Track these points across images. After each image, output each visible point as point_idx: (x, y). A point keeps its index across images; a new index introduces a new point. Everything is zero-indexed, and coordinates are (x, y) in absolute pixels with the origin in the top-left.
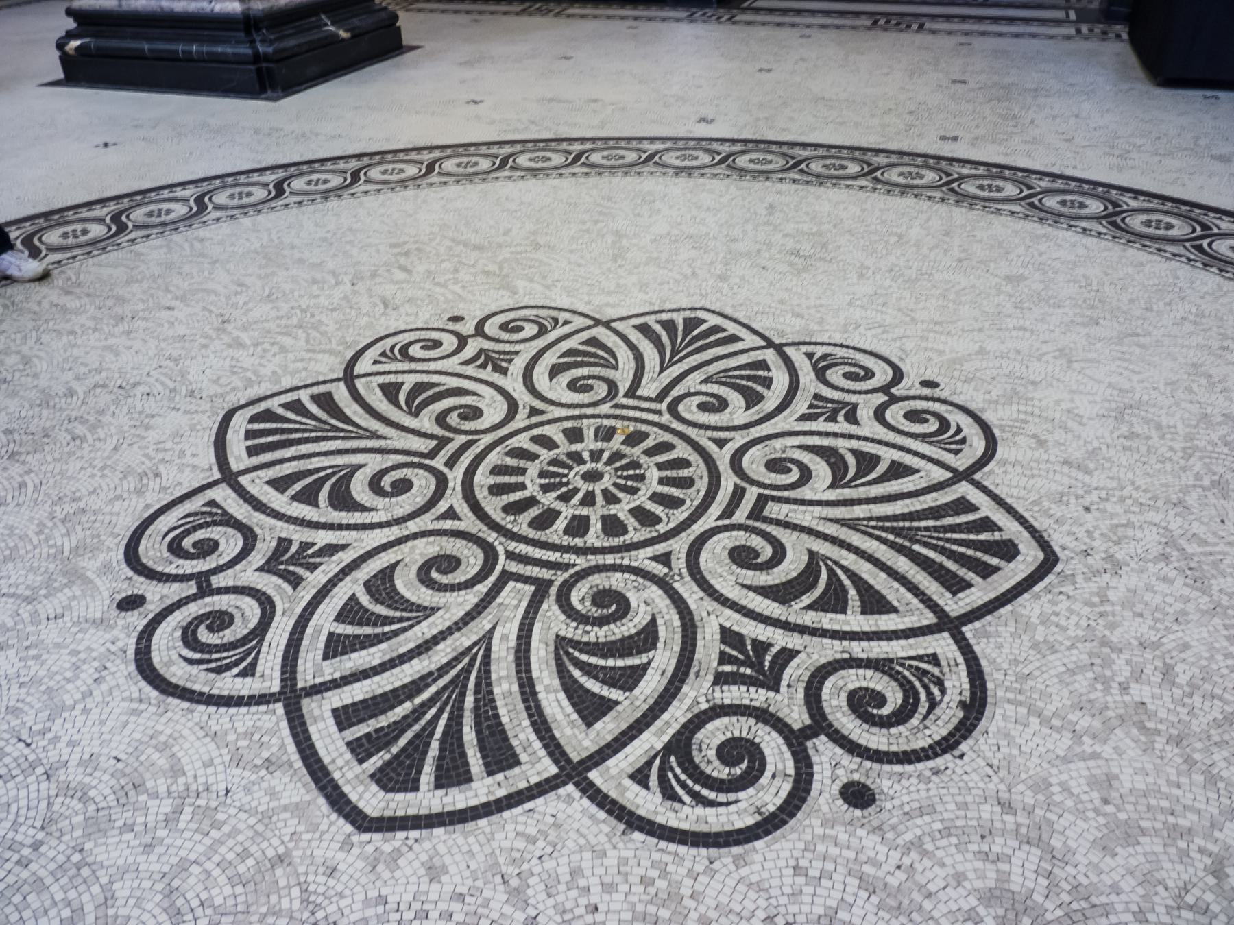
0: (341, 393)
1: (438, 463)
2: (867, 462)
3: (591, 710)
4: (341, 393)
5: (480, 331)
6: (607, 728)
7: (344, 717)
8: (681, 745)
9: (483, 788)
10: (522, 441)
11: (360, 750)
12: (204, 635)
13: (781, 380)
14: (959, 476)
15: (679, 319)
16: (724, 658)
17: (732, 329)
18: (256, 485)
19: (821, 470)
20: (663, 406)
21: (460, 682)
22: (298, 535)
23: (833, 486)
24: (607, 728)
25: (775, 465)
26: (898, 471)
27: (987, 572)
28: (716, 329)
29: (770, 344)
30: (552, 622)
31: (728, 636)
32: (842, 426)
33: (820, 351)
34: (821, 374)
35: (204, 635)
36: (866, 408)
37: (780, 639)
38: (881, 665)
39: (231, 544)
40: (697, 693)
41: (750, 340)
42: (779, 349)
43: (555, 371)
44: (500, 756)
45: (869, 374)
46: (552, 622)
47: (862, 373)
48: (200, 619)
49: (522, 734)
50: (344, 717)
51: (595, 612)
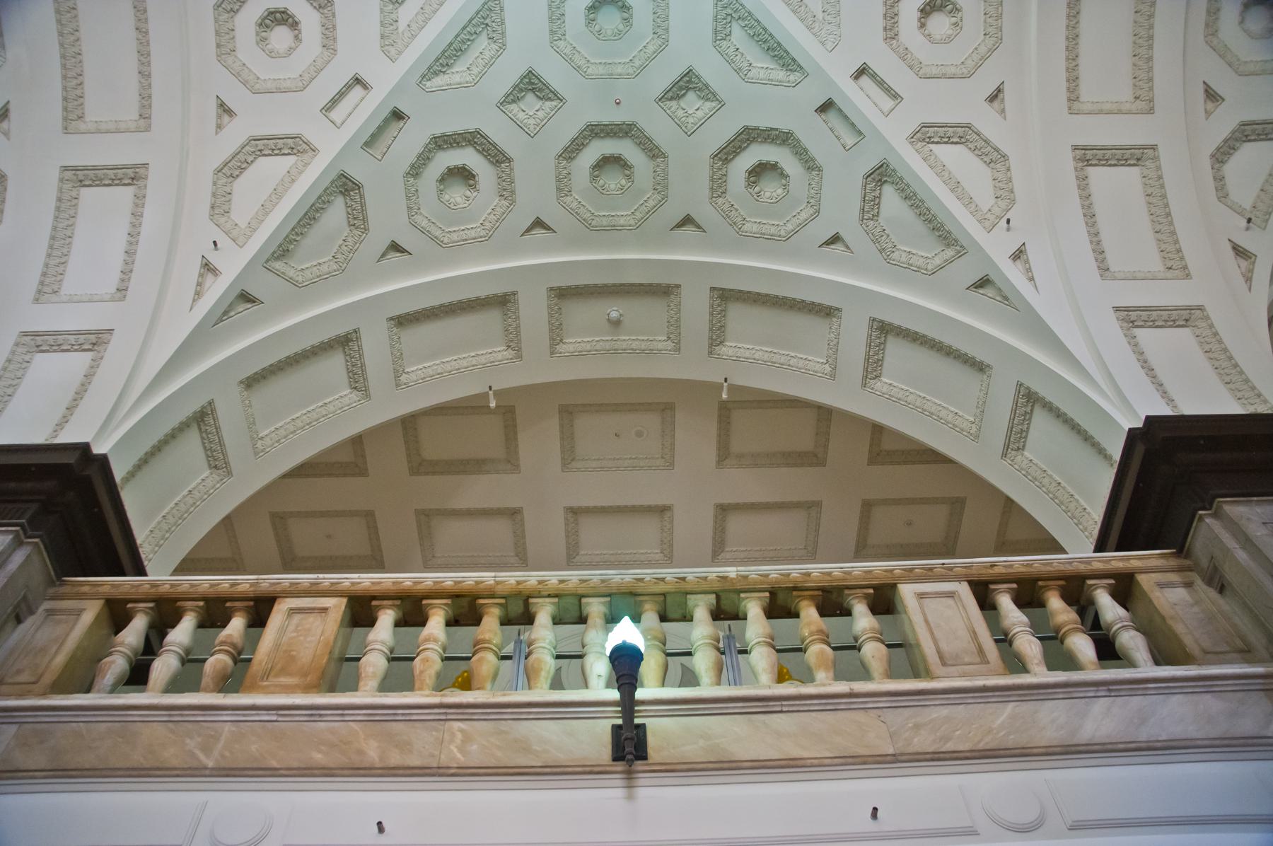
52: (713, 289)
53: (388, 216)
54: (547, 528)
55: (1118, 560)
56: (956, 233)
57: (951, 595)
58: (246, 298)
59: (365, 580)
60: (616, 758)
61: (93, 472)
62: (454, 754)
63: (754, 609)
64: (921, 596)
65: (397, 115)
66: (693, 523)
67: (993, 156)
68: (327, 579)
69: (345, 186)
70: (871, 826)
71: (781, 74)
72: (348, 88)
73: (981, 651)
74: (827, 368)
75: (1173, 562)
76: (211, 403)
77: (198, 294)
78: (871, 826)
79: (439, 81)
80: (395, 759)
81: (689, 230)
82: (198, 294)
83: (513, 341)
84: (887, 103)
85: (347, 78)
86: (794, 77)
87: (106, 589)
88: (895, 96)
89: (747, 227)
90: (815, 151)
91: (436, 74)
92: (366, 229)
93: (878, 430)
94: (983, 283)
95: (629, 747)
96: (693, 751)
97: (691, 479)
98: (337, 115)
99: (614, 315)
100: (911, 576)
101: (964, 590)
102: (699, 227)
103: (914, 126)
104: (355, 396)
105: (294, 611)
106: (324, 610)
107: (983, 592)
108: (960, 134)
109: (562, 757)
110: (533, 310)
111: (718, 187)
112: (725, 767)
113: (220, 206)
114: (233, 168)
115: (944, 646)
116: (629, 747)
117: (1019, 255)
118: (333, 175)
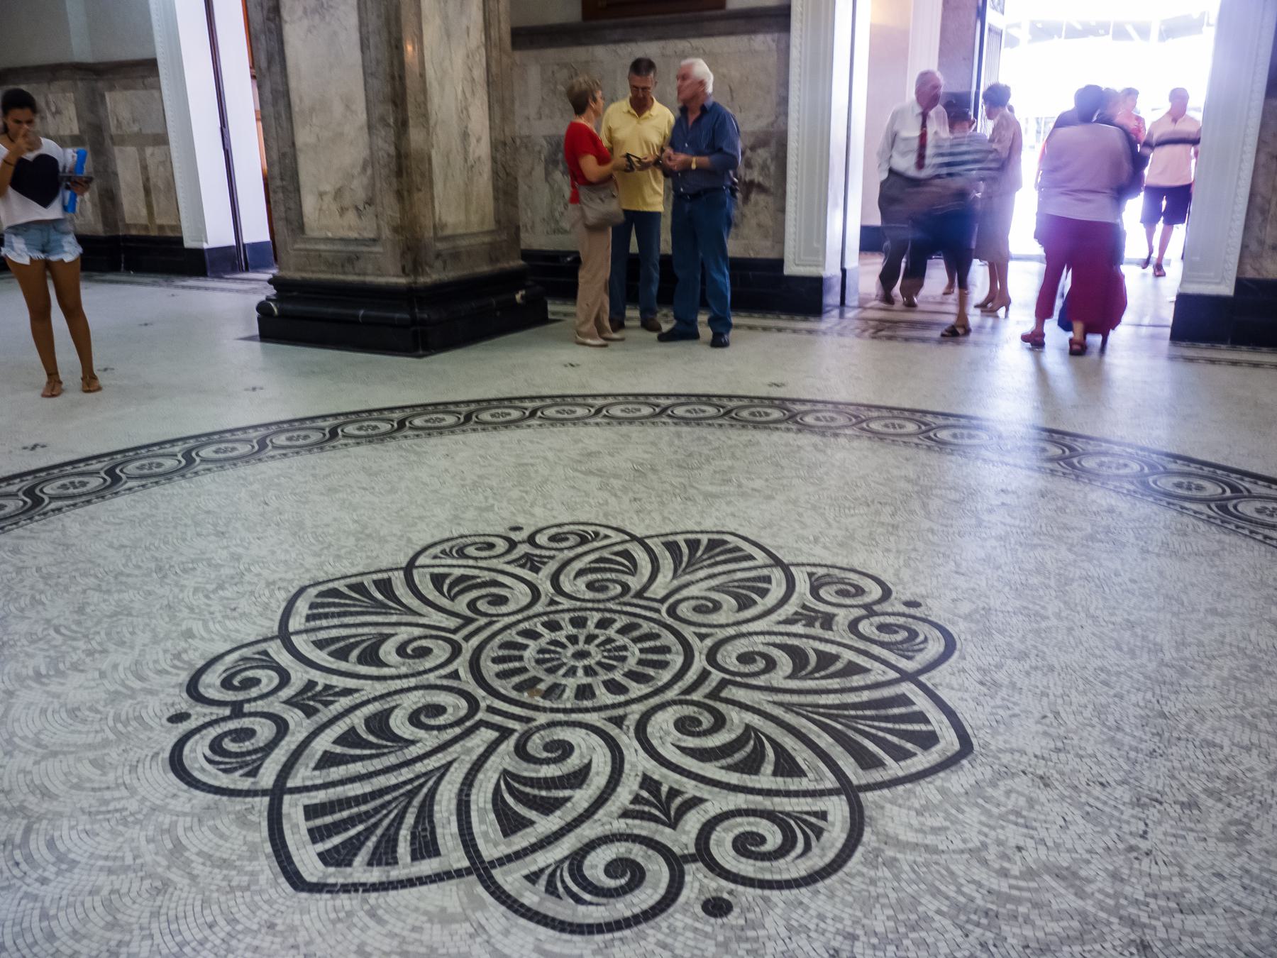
0: (398, 579)
1: (457, 637)
2: (826, 660)
3: (510, 824)
4: (398, 579)
5: (531, 540)
6: (521, 840)
7: (311, 812)
8: (577, 859)
9: (406, 867)
10: (637, 689)
11: (316, 835)
12: (229, 745)
14: (905, 676)
15: (704, 539)
16: (637, 799)
18: (299, 642)
19: (785, 663)
20: (664, 608)
21: (411, 794)
22: (321, 679)
23: (791, 676)
24: (521, 840)
26: (852, 669)
27: (900, 755)
30: (504, 758)
31: (648, 782)
33: (821, 571)
34: (814, 591)
35: (229, 745)
36: (843, 617)
37: (691, 788)
38: (770, 815)
39: (268, 679)
40: (607, 821)
41: (761, 558)
43: (580, 573)
44: (426, 846)
46: (504, 758)
47: (852, 590)
48: (225, 734)
49: (447, 833)
50: (311, 812)
51: (545, 755)
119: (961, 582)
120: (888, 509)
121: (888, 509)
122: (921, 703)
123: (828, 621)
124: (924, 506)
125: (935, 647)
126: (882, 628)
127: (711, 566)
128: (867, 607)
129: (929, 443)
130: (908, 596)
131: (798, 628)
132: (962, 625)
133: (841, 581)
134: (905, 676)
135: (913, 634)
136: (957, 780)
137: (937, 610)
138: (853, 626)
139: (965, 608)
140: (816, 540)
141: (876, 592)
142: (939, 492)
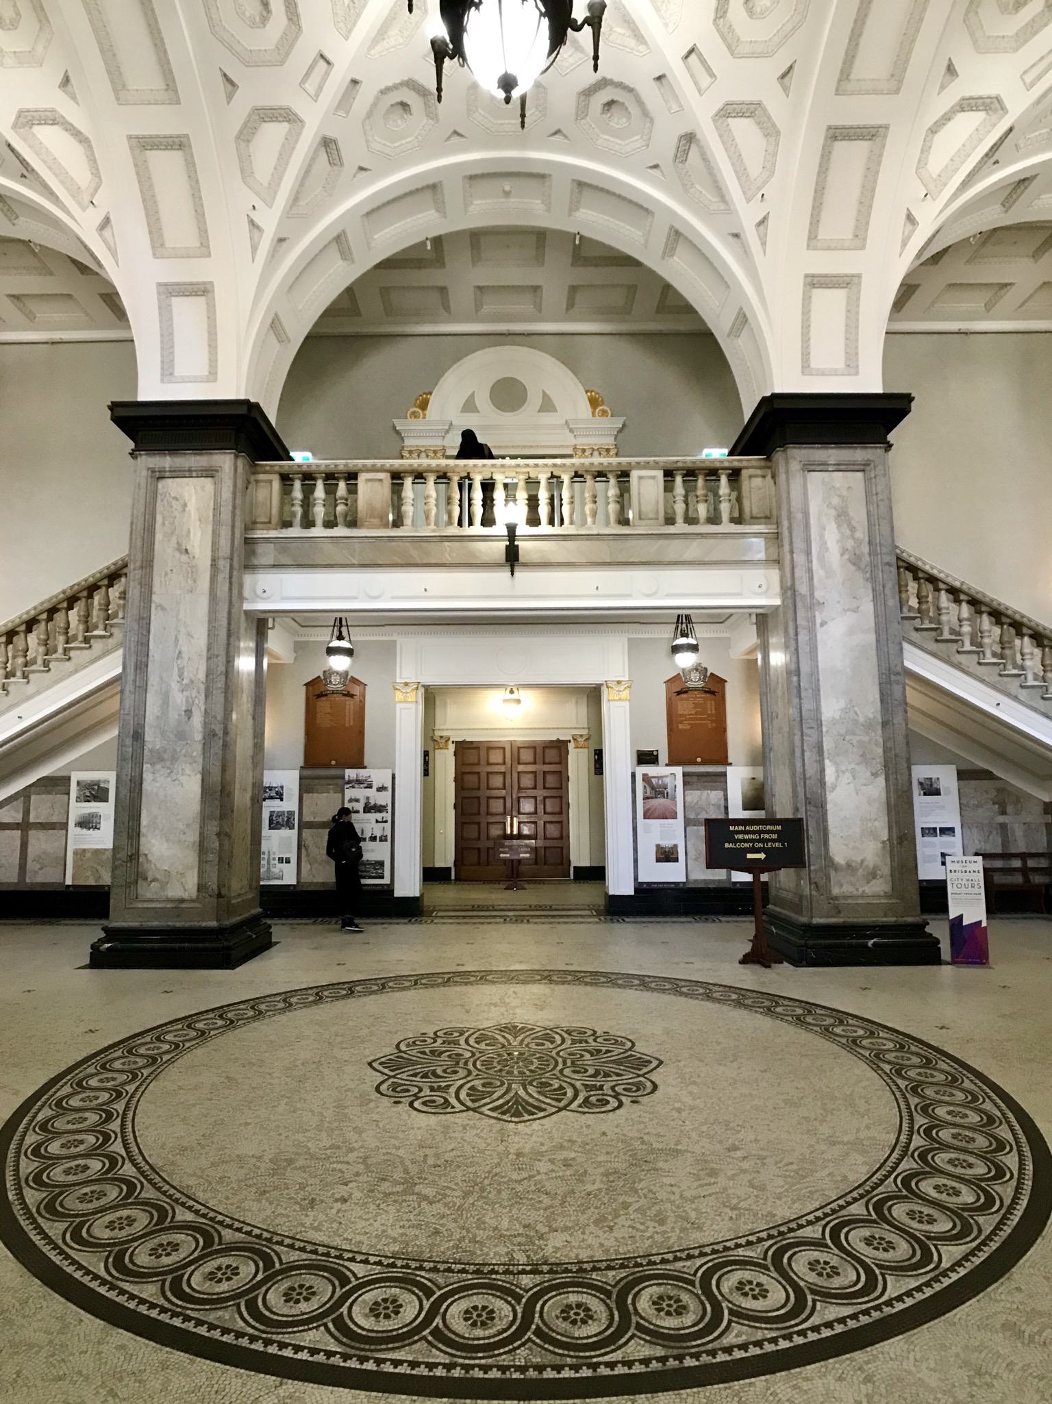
2: (425, 1076)
13: (463, 1095)
17: (495, 1115)
25: (456, 1072)
28: (504, 1113)
29: (474, 1110)
32: (435, 1085)
33: (449, 1110)
34: (446, 1100)
41: (484, 1109)
42: (468, 1109)
45: (424, 1103)
52: (573, 180)
53: (352, 153)
54: (462, 296)
55: (737, 461)
56: (727, 198)
57: (654, 478)
58: (281, 240)
59: (397, 463)
60: (507, 560)
61: (255, 414)
62: (449, 560)
63: (566, 478)
64: (640, 478)
65: (355, 82)
66: (554, 294)
67: (770, 131)
68: (379, 462)
69: (327, 143)
70: (596, 592)
71: (632, 43)
72: (315, 62)
73: (657, 512)
74: (642, 241)
75: (763, 463)
76: (276, 315)
77: (254, 249)
78: (596, 592)
79: (378, 48)
80: (425, 561)
81: (558, 138)
82: (254, 249)
83: (440, 207)
84: (705, 81)
85: (314, 54)
86: (642, 48)
87: (277, 469)
88: (712, 75)
89: (599, 142)
90: (650, 105)
91: (378, 42)
92: (342, 165)
93: (667, 288)
94: (736, 236)
95: (512, 557)
96: (535, 558)
97: (553, 277)
98: (310, 86)
99: (507, 188)
100: (639, 466)
101: (660, 474)
102: (566, 137)
103: (720, 105)
104: (345, 264)
105: (368, 480)
106: (380, 480)
107: (669, 474)
108: (751, 110)
109: (485, 559)
110: (453, 191)
111: (582, 112)
112: (545, 565)
113: (246, 172)
114: (246, 134)
115: (643, 509)
116: (512, 557)
117: (763, 222)
118: (318, 139)
119: (375, 1117)
120: (431, 1161)
121: (431, 1161)
122: (386, 1071)
123: (432, 1089)
124: (406, 1171)
125: (383, 1088)
126: (408, 1091)
127: (508, 1102)
128: (415, 1095)
129: (423, 1277)
130: (400, 1106)
131: (443, 1084)
132: (373, 1097)
133: (436, 1107)
134: (394, 1077)
135: (394, 1090)
136: (372, 1058)
137: (386, 1102)
138: (421, 1090)
139: (372, 1105)
140: (465, 1128)
141: (416, 1104)
142: (399, 1188)
